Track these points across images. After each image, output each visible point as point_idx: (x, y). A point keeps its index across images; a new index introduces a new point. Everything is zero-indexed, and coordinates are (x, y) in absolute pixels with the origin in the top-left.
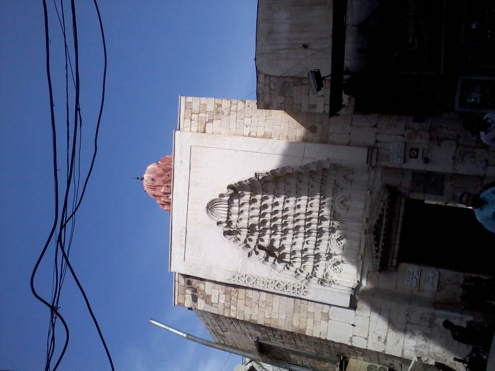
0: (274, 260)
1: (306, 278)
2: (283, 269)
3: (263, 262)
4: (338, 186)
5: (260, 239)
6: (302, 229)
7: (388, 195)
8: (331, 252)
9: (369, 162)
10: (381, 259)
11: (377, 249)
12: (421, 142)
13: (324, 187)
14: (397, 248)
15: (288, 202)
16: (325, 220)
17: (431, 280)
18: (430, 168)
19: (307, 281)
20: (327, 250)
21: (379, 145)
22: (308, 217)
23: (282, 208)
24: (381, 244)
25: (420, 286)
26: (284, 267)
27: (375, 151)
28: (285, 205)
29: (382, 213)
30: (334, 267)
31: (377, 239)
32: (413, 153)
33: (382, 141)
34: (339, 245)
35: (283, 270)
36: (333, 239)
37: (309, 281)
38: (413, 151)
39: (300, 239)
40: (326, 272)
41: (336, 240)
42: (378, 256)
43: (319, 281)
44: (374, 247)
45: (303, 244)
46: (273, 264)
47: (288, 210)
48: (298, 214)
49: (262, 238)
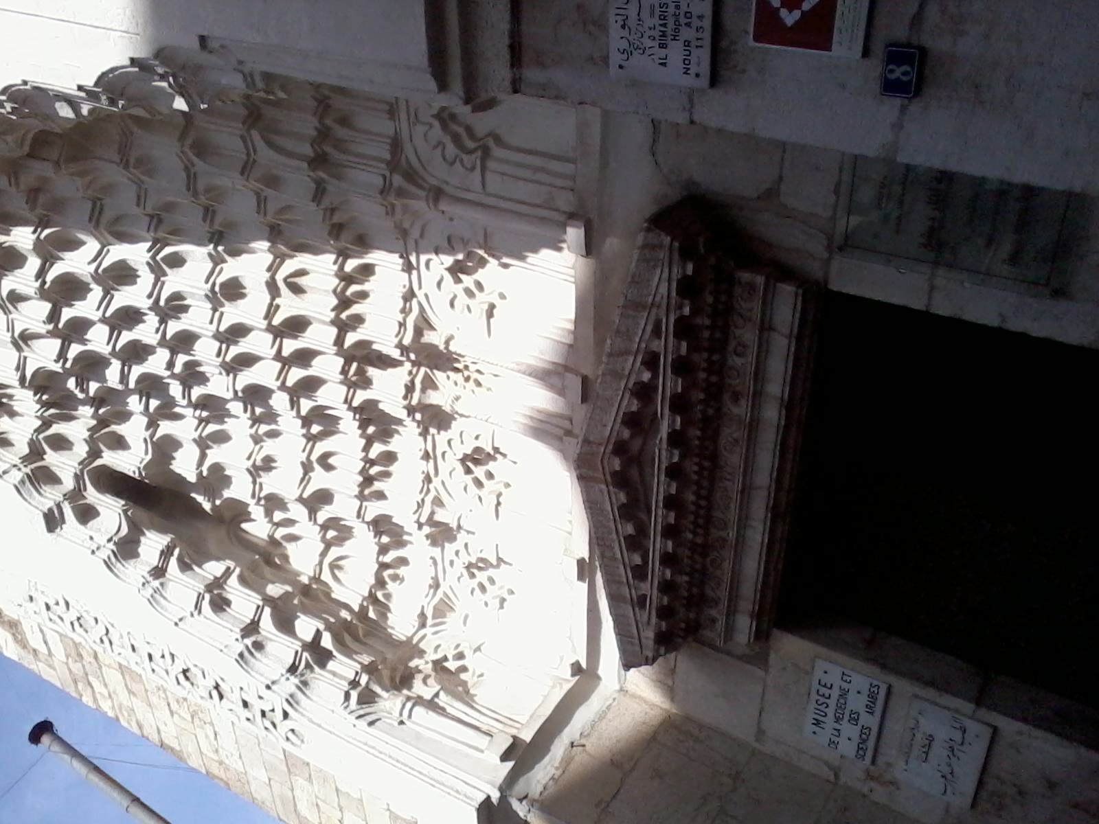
0: (162, 552)
1: (293, 669)
2: (193, 608)
3: (108, 564)
4: (411, 176)
5: (105, 436)
6: (280, 401)
7: (676, 273)
8: (440, 516)
10: (665, 613)
11: (637, 560)
13: (332, 186)
14: (752, 566)
15: (176, 261)
16: (385, 362)
17: (939, 751)
18: (936, 138)
19: (294, 680)
20: (420, 505)
22: (290, 346)
23: (150, 296)
24: (657, 545)
25: (881, 761)
26: (200, 597)
28: (162, 279)
29: (646, 376)
30: (473, 576)
31: (633, 510)
34: (479, 484)
35: (192, 615)
36: (443, 454)
37: (305, 683)
39: (289, 444)
40: (440, 594)
41: (463, 460)
42: (645, 596)
43: (354, 684)
44: (617, 549)
45: (307, 468)
46: (151, 579)
47: (185, 309)
48: (238, 332)
49: (114, 433)
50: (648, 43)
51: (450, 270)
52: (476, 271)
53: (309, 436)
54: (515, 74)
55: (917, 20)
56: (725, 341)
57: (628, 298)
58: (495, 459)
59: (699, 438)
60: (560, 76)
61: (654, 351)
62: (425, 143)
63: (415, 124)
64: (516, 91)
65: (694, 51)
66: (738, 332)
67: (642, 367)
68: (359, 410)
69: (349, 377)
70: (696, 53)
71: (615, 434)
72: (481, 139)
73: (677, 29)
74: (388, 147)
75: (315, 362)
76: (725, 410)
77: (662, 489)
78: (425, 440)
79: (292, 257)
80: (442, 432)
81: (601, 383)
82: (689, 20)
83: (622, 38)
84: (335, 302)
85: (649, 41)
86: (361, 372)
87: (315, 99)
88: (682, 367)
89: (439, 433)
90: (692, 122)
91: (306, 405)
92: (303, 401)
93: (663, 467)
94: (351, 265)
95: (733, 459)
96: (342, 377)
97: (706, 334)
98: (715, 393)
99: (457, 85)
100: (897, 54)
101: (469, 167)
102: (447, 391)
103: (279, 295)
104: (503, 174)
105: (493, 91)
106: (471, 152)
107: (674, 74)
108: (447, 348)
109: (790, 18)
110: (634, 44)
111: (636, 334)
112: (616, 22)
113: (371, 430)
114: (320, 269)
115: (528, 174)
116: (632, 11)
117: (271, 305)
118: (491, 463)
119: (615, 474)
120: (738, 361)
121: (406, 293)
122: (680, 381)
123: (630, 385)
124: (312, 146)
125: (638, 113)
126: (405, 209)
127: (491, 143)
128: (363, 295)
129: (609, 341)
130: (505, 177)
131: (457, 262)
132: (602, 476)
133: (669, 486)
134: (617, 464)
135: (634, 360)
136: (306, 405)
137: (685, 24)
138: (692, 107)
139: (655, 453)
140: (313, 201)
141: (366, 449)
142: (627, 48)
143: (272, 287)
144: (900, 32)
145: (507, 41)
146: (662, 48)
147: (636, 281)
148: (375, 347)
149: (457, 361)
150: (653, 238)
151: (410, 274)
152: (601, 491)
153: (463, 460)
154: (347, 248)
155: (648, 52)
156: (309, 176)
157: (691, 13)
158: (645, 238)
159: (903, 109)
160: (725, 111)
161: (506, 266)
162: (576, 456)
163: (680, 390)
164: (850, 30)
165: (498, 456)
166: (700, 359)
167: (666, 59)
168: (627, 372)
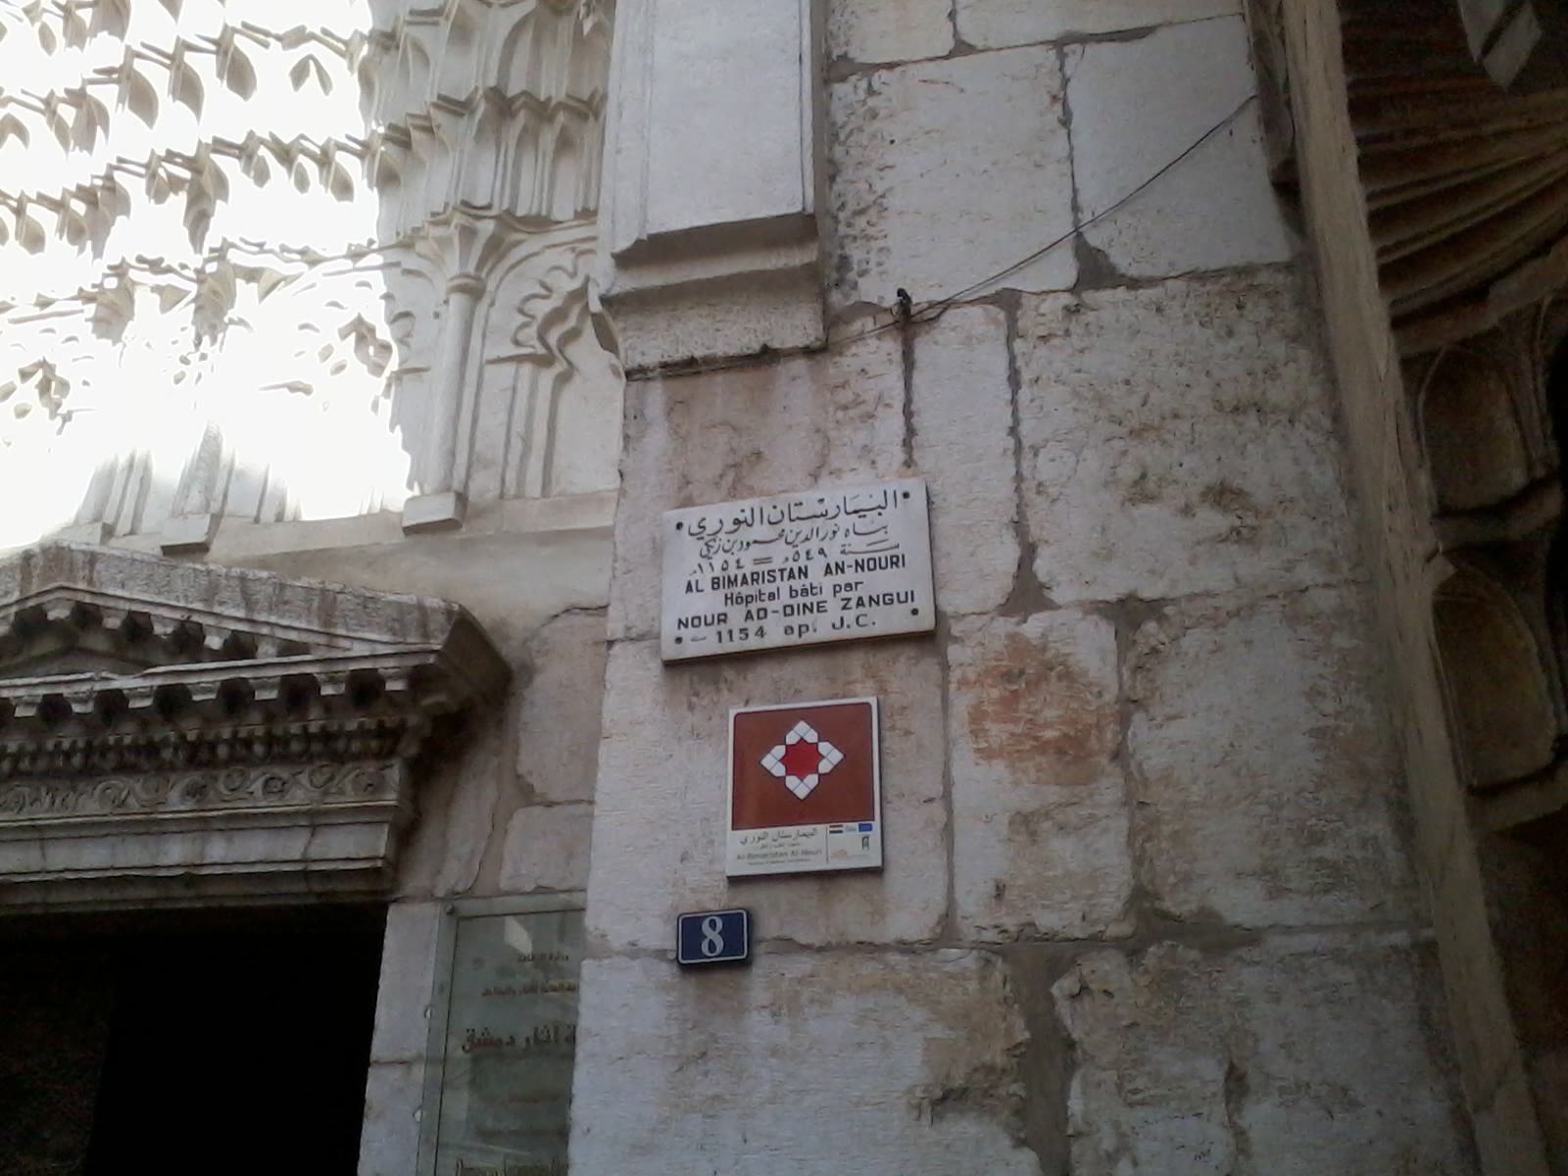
4: (495, 249)
9: (653, 278)
12: (969, 832)
13: (467, 127)
16: (198, 220)
21: (873, 355)
22: (204, 66)
27: (796, 326)
29: (214, 642)
32: (801, 759)
33: (918, 378)
36: (51, 331)
38: (824, 748)
50: (718, 561)
51: (359, 321)
52: (363, 362)
53: (54, 102)
54: (652, 371)
55: (788, 946)
56: (285, 759)
57: (340, 597)
58: (53, 415)
59: (119, 741)
60: (657, 438)
61: (257, 648)
62: (551, 269)
63: (573, 250)
64: (629, 374)
65: (715, 628)
66: (304, 778)
67: (227, 635)
68: (109, 184)
69: (164, 164)
70: (709, 633)
71: (111, 603)
72: (561, 352)
73: (740, 600)
74: (534, 211)
75: (181, 107)
76: (173, 777)
77: (20, 692)
78: (73, 299)
79: (351, 68)
80: (90, 325)
81: (195, 570)
82: (755, 617)
83: (721, 522)
84: (286, 140)
85: (721, 562)
86: (175, 184)
87: (592, 96)
88: (235, 697)
89: (87, 320)
90: (611, 643)
91: (107, 95)
92: (115, 89)
93: (64, 691)
94: (351, 166)
95: (90, 804)
96: (163, 154)
97: (295, 728)
98: (199, 756)
99: (628, 283)
100: (738, 928)
101: (521, 337)
102: (159, 326)
103: (285, 47)
104: (514, 390)
105: (625, 340)
106: (542, 339)
107: (679, 605)
108: (231, 321)
109: (773, 762)
110: (715, 540)
111: (282, 616)
112: (743, 511)
113: (79, 207)
114: (339, 113)
115: (519, 426)
116: (761, 531)
117: (267, 34)
118: (46, 411)
119: (40, 612)
120: (257, 787)
121: (315, 253)
122: (213, 696)
123: (195, 618)
124: (524, 93)
125: (615, 561)
126: (444, 243)
127: (559, 367)
128: (302, 183)
129: (264, 574)
130: (509, 393)
131: (372, 330)
132: (34, 590)
133: (28, 704)
134: (58, 613)
135: (239, 620)
136: (107, 95)
137: (749, 612)
138: (632, 639)
139: (83, 673)
140: (440, 97)
141: (42, 199)
142: (709, 530)
143: (299, 36)
144: (769, 927)
145: (698, 353)
146: (713, 583)
147: (367, 602)
148: (219, 203)
149: (214, 340)
150: (438, 622)
151: (345, 257)
152: (7, 593)
153: (43, 364)
154: (374, 156)
155: (705, 563)
156: (477, 88)
157: (766, 616)
158: (434, 610)
159: (660, 954)
160: (632, 690)
161: (375, 407)
162: (65, 544)
163: (196, 698)
164: (764, 851)
165: (59, 420)
166: (253, 724)
167: (698, 591)
168: (217, 609)
